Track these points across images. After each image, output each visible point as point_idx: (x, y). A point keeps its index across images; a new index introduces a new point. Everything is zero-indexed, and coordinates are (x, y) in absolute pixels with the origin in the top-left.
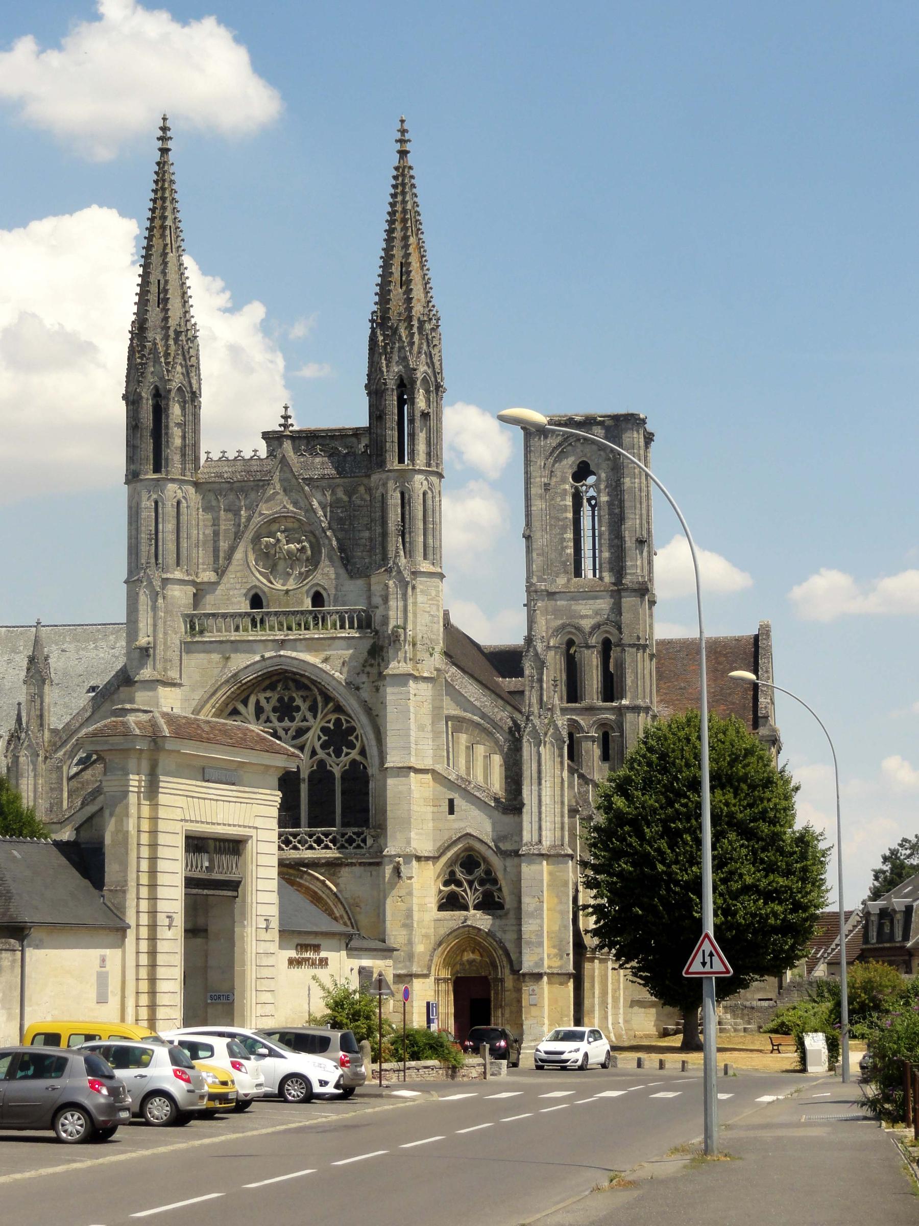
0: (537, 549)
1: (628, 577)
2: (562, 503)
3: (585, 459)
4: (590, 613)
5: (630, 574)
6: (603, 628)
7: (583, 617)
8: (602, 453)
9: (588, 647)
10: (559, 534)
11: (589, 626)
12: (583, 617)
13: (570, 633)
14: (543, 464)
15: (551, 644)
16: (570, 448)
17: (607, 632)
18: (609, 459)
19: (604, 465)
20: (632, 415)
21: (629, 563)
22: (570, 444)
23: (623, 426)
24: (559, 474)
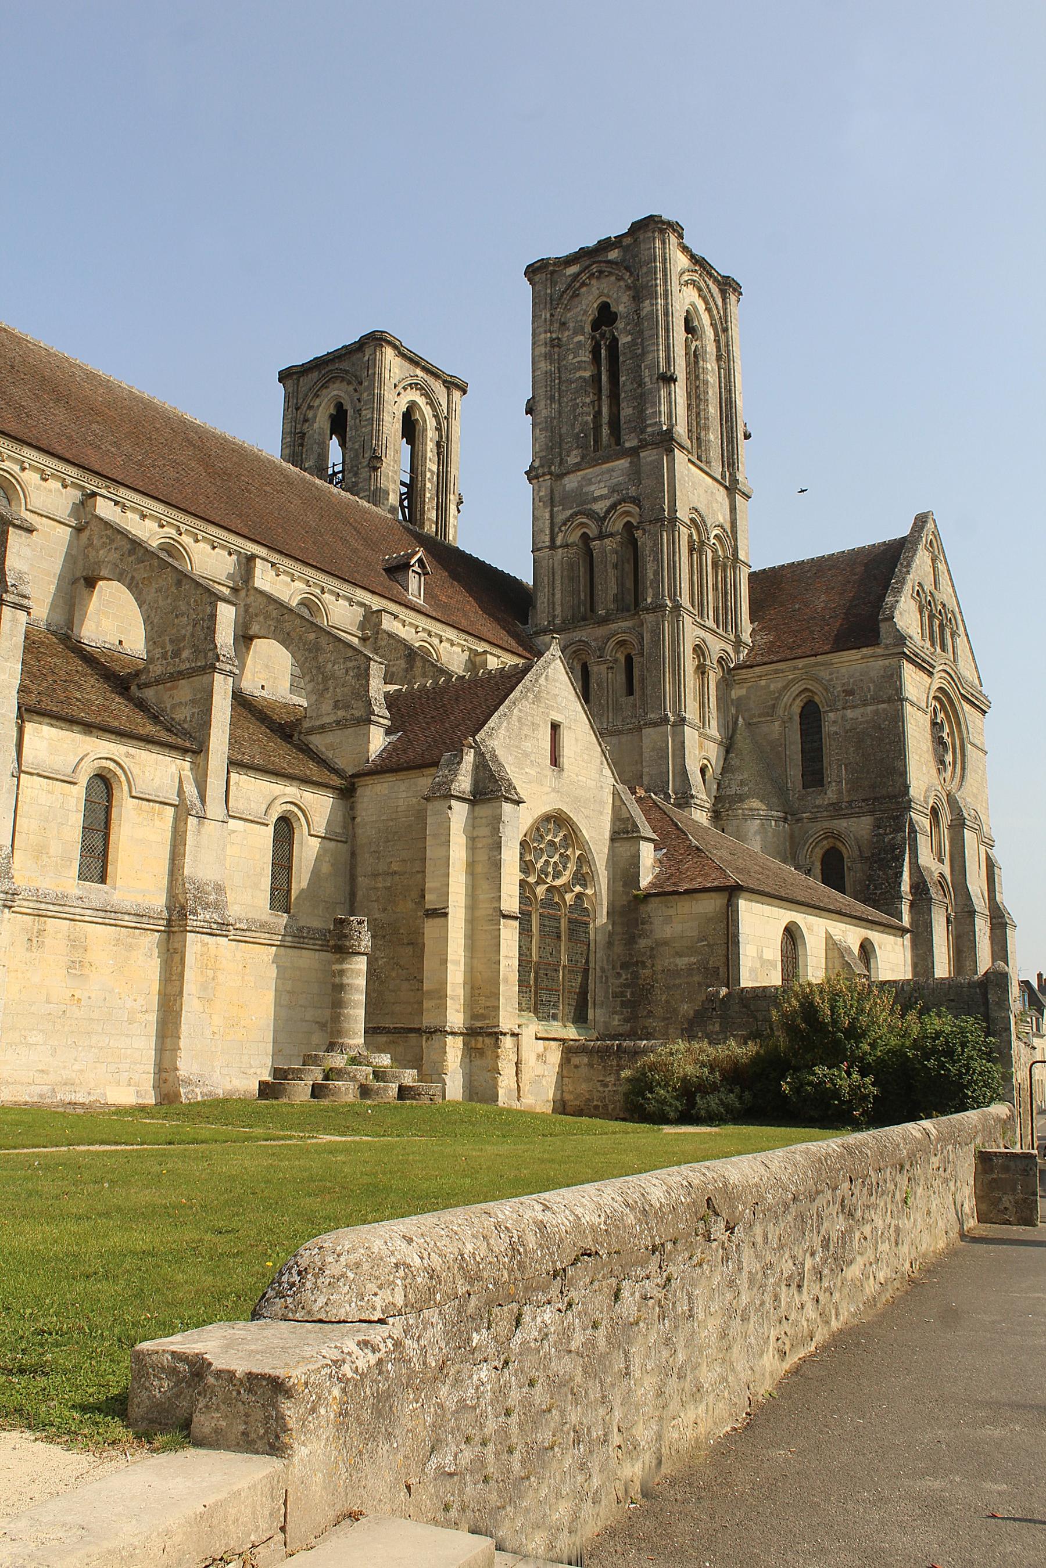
0: (540, 424)
1: (649, 429)
2: (575, 360)
3: (604, 299)
4: (605, 491)
5: (650, 425)
6: (621, 508)
7: (596, 500)
8: (622, 283)
9: (601, 537)
10: (571, 400)
11: (604, 510)
12: (596, 500)
13: (582, 524)
14: (548, 315)
15: (558, 542)
16: (584, 289)
17: (627, 513)
18: (628, 288)
19: (625, 298)
20: (651, 217)
21: (649, 411)
22: (583, 284)
23: (641, 237)
24: (572, 325)
